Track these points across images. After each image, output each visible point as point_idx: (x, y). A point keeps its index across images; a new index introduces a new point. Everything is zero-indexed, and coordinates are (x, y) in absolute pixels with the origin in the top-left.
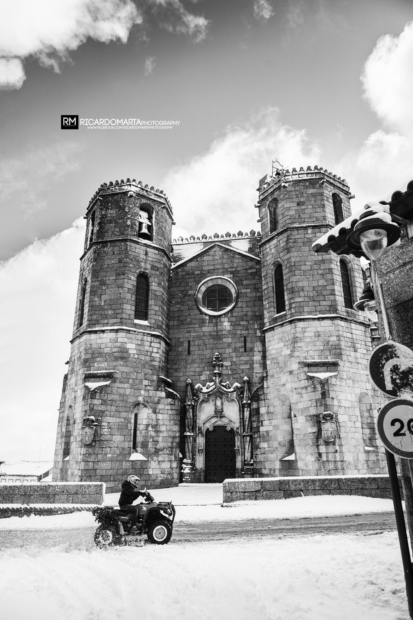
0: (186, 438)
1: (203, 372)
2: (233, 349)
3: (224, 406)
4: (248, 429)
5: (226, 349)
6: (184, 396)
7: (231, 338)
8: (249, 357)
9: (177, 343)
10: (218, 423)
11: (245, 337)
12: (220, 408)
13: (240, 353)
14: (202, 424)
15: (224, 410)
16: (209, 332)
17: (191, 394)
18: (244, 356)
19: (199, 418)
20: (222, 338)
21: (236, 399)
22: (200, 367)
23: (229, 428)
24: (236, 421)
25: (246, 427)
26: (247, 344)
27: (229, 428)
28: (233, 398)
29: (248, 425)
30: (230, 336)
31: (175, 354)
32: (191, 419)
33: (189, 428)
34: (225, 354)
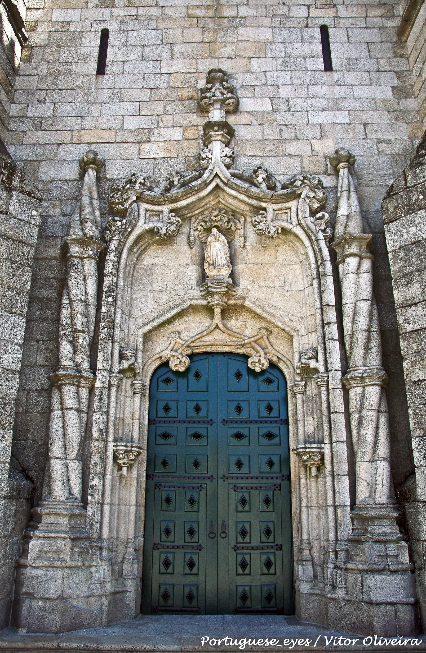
0: (59, 388)
1: (156, 132)
2: (280, 61)
3: (240, 267)
4: (367, 348)
5: (250, 58)
6: (64, 215)
7: (270, 30)
8: (344, 88)
9: (56, 36)
10: (210, 337)
11: (324, 30)
12: (225, 272)
13: (310, 73)
14: (141, 340)
15: (243, 282)
16: (184, 10)
17: (96, 203)
18: (324, 84)
19: (126, 310)
20: (236, 27)
21: (298, 231)
22: (143, 112)
23: (263, 361)
24: (296, 325)
25: (360, 339)
26: (333, 47)
27: (263, 361)
28: (288, 226)
29: (369, 331)
30: (267, 21)
31: (45, 72)
32: (86, 303)
33: (73, 343)
34: (248, 75)
